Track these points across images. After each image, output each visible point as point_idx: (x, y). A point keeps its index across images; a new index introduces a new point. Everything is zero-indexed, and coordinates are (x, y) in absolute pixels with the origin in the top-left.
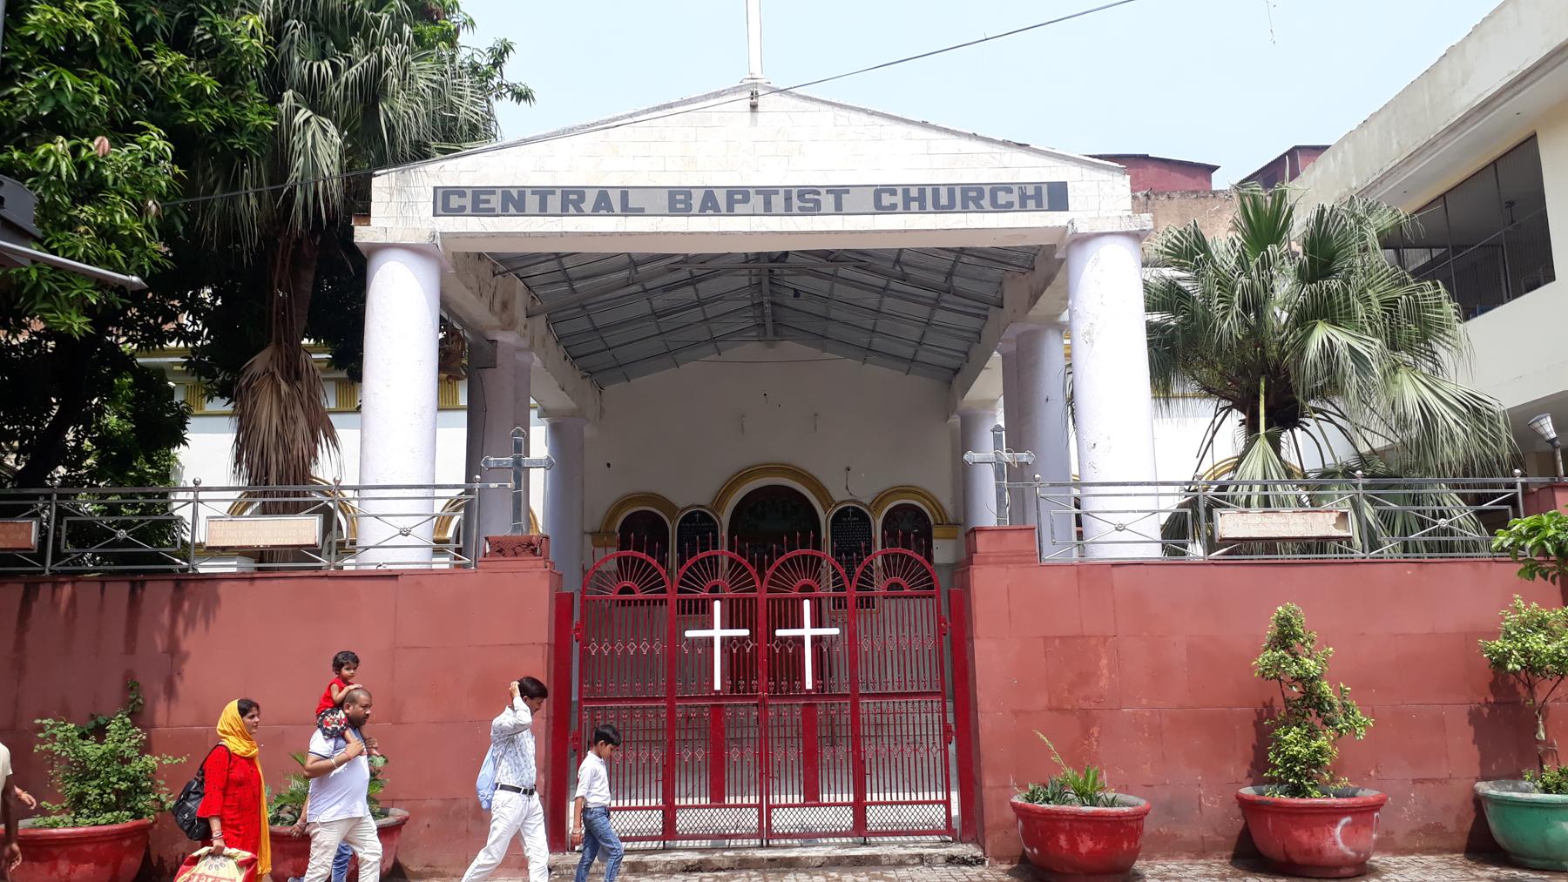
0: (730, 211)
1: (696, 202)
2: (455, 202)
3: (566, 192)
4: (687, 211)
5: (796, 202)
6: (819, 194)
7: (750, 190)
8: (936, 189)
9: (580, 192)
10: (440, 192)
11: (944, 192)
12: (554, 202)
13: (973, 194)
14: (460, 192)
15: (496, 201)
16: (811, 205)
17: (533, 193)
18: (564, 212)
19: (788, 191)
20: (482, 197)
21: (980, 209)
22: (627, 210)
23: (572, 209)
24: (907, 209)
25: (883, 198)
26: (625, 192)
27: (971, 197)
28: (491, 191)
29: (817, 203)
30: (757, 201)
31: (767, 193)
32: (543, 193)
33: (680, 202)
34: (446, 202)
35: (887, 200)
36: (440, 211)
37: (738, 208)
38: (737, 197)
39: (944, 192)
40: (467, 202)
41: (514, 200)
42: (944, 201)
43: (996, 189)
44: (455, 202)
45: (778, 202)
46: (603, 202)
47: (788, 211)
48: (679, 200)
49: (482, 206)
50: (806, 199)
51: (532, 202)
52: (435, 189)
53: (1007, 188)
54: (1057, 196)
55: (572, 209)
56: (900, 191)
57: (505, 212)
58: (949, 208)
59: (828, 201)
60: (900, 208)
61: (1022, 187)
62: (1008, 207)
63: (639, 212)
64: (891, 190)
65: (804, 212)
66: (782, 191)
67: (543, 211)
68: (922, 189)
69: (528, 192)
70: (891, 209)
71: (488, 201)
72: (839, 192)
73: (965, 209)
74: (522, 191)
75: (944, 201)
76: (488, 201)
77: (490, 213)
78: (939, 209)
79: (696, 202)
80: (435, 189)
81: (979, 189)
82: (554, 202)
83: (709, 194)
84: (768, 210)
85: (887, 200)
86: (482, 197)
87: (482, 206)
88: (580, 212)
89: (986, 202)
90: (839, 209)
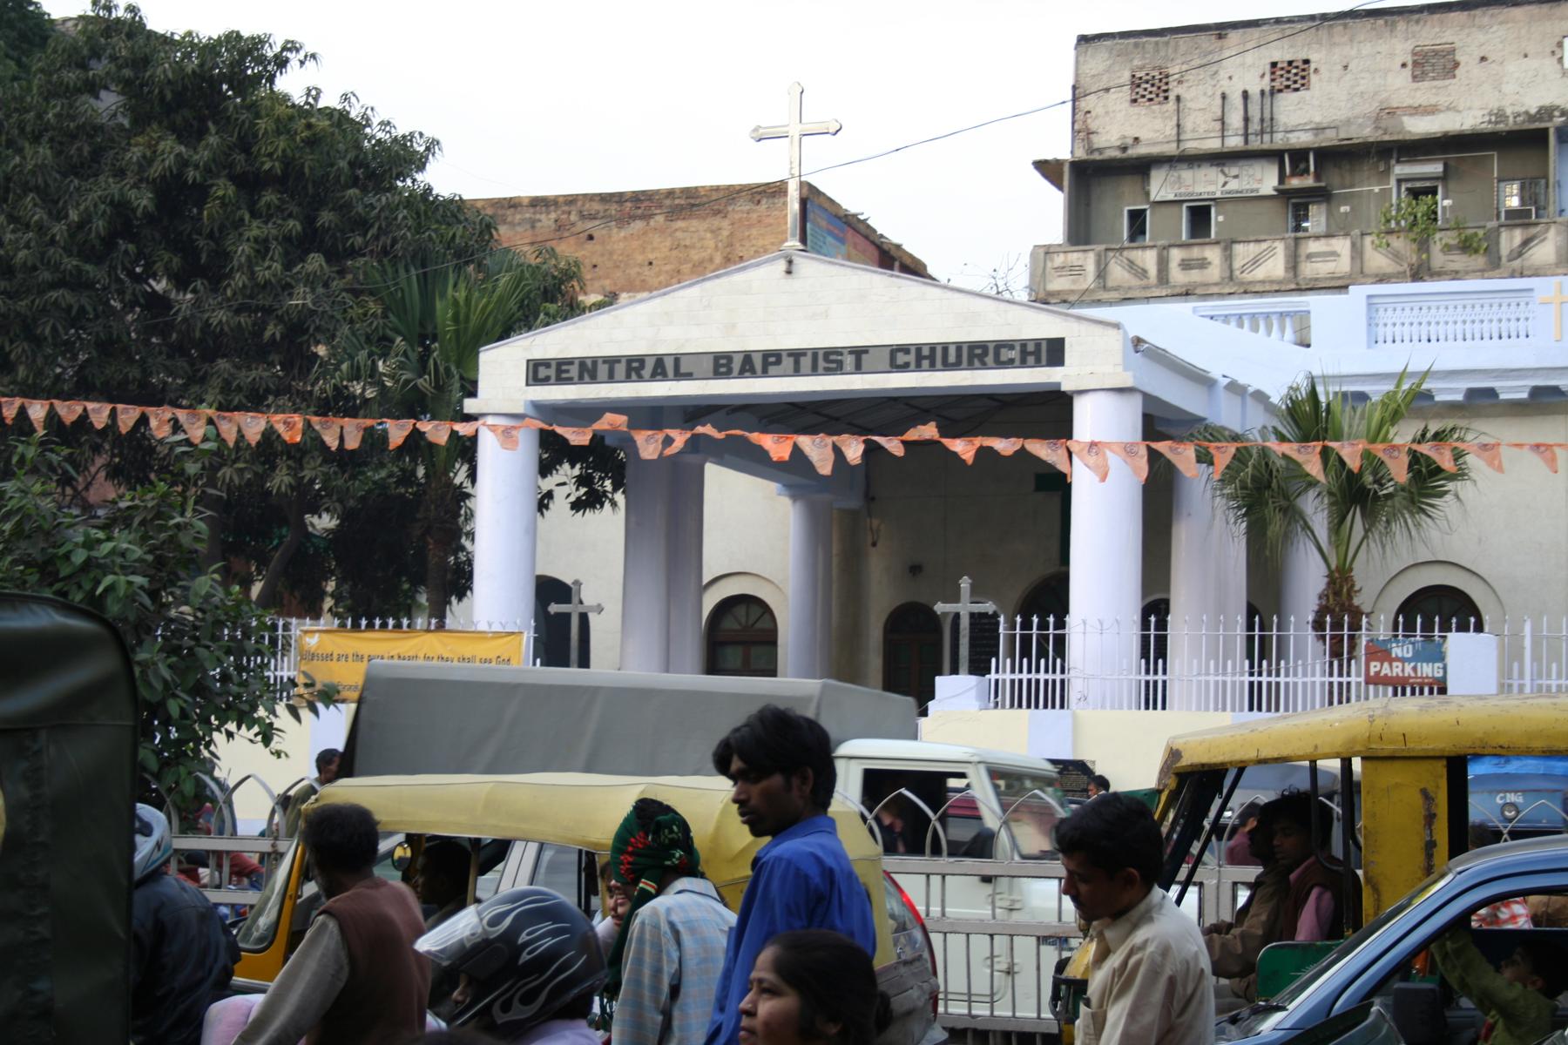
0: (765, 373)
1: (736, 365)
2: (543, 372)
3: (630, 360)
4: (727, 374)
5: (821, 364)
6: (841, 354)
7: (784, 354)
8: (945, 347)
9: (641, 360)
10: (531, 364)
11: (952, 351)
12: (620, 369)
13: (978, 351)
14: (546, 363)
15: (574, 371)
16: (834, 365)
17: (605, 362)
18: (628, 379)
19: (815, 353)
20: (564, 367)
21: (984, 366)
22: (680, 375)
23: (634, 376)
24: (919, 368)
25: (900, 357)
26: (677, 359)
27: (978, 354)
28: (570, 361)
29: (840, 364)
30: (788, 362)
31: (797, 355)
32: (612, 361)
33: (723, 365)
34: (538, 372)
35: (901, 358)
36: (531, 382)
37: (772, 369)
38: (772, 359)
39: (952, 351)
40: (552, 372)
41: (588, 369)
42: (952, 358)
43: (1001, 345)
44: (543, 372)
45: (806, 362)
46: (660, 367)
47: (814, 371)
48: (722, 365)
49: (564, 375)
50: (829, 360)
51: (603, 370)
52: (528, 361)
53: (1009, 345)
54: (1054, 351)
55: (634, 376)
56: (913, 350)
57: (581, 380)
58: (957, 366)
59: (849, 361)
60: (913, 366)
61: (1024, 344)
62: (1009, 364)
63: (689, 376)
64: (904, 349)
65: (829, 371)
66: (810, 354)
67: (611, 378)
68: (933, 347)
69: (600, 361)
70: (904, 367)
71: (567, 371)
72: (859, 353)
73: (971, 366)
74: (595, 360)
75: (952, 358)
76: (567, 371)
77: (569, 381)
78: (947, 366)
79: (736, 366)
80: (528, 361)
81: (983, 346)
82: (620, 369)
83: (747, 357)
84: (797, 371)
85: (901, 358)
86: (564, 367)
87: (564, 375)
88: (640, 379)
89: (990, 359)
90: (858, 369)
